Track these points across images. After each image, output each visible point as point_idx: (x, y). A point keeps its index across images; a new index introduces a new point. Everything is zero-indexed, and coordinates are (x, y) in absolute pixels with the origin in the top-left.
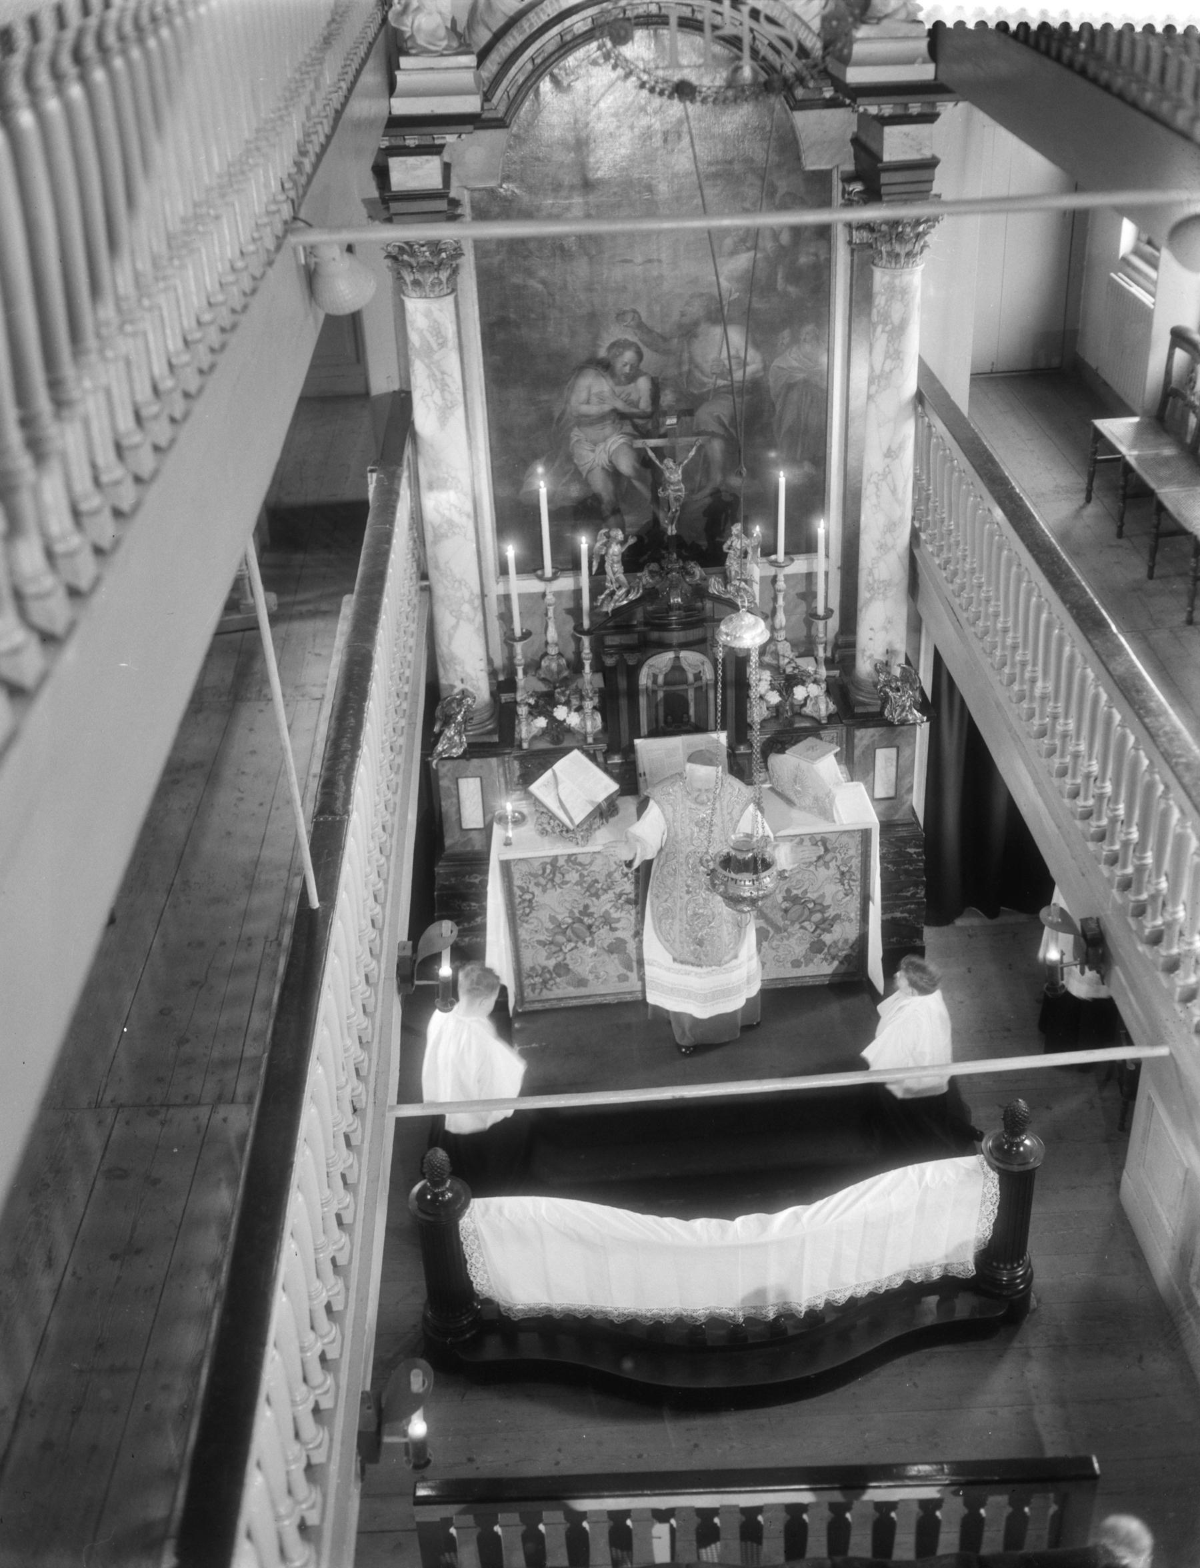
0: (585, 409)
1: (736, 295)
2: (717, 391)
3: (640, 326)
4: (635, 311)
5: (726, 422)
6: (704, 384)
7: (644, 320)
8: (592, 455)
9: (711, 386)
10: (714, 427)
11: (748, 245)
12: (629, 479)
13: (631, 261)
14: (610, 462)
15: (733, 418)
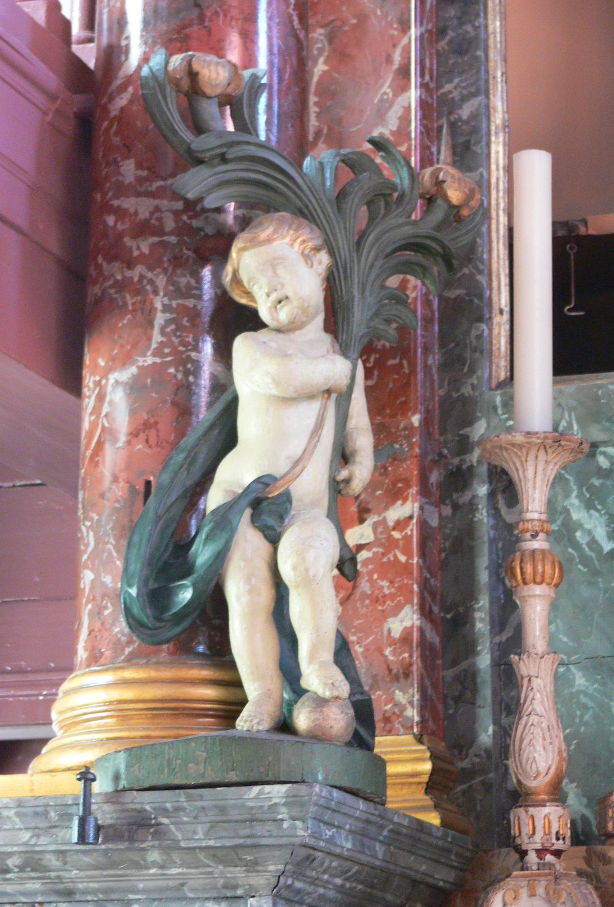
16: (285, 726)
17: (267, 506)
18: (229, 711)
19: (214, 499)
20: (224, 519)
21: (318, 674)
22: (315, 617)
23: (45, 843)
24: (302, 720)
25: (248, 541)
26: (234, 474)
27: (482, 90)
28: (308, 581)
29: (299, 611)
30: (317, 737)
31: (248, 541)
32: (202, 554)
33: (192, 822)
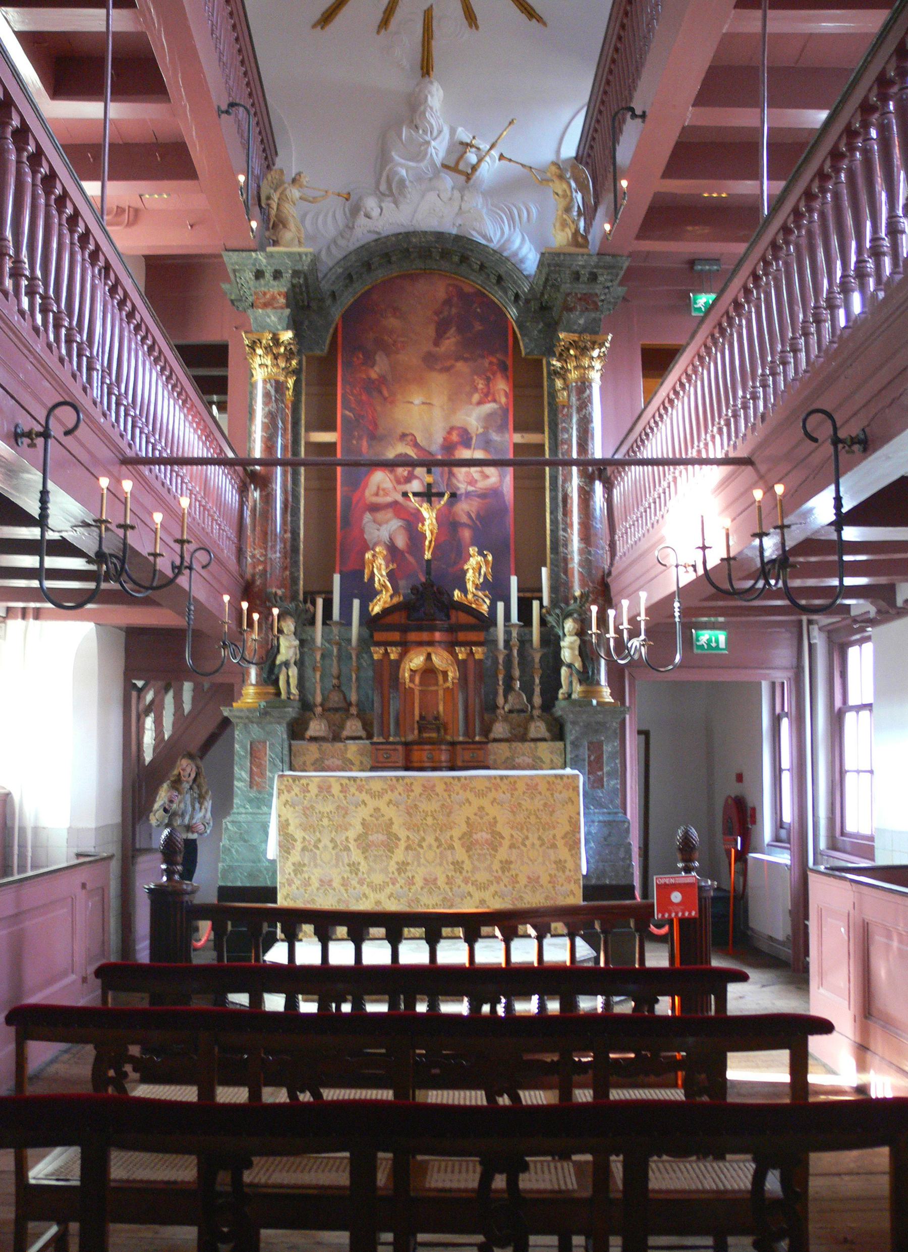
0: (375, 500)
1: (481, 430)
2: (468, 494)
3: (416, 445)
4: (413, 435)
5: (473, 515)
6: (458, 489)
7: (419, 440)
8: (377, 533)
9: (462, 491)
10: (464, 519)
11: (489, 399)
12: (402, 552)
13: (412, 403)
14: (391, 539)
15: (478, 515)
16: (289, 698)
17: (286, 664)
18: (278, 694)
19: (278, 662)
20: (280, 665)
21: (294, 690)
22: (293, 682)
23: (251, 716)
24: (292, 697)
25: (284, 669)
26: (280, 659)
27: (298, 571)
28: (293, 676)
29: (291, 680)
30: (294, 700)
31: (284, 669)
32: (276, 671)
33: (275, 713)
